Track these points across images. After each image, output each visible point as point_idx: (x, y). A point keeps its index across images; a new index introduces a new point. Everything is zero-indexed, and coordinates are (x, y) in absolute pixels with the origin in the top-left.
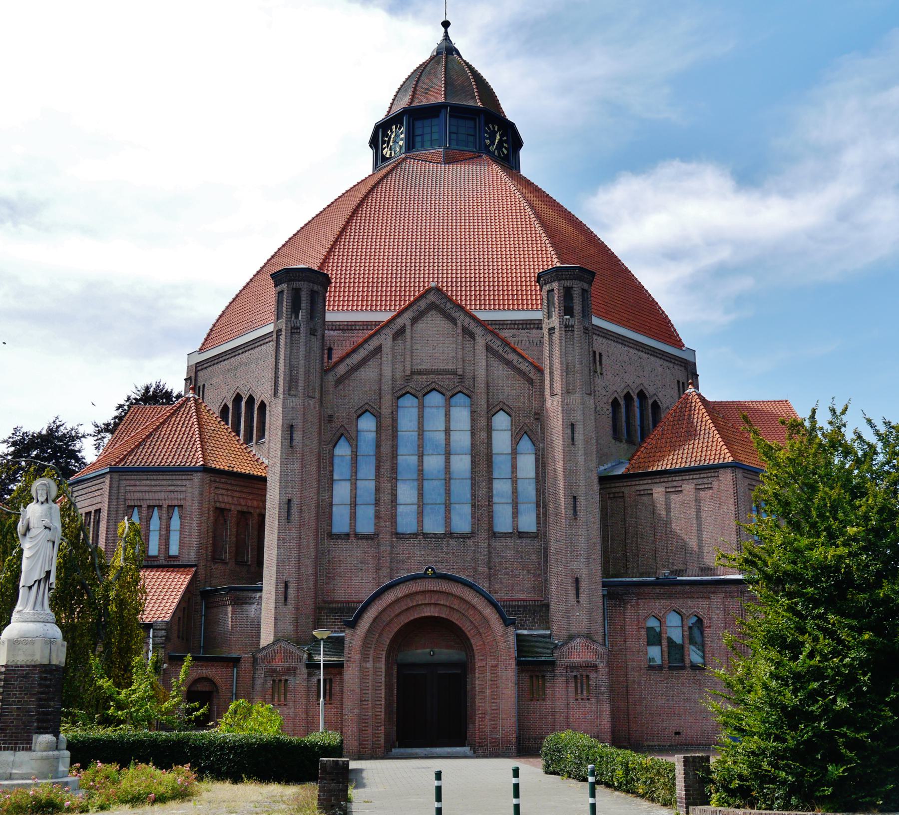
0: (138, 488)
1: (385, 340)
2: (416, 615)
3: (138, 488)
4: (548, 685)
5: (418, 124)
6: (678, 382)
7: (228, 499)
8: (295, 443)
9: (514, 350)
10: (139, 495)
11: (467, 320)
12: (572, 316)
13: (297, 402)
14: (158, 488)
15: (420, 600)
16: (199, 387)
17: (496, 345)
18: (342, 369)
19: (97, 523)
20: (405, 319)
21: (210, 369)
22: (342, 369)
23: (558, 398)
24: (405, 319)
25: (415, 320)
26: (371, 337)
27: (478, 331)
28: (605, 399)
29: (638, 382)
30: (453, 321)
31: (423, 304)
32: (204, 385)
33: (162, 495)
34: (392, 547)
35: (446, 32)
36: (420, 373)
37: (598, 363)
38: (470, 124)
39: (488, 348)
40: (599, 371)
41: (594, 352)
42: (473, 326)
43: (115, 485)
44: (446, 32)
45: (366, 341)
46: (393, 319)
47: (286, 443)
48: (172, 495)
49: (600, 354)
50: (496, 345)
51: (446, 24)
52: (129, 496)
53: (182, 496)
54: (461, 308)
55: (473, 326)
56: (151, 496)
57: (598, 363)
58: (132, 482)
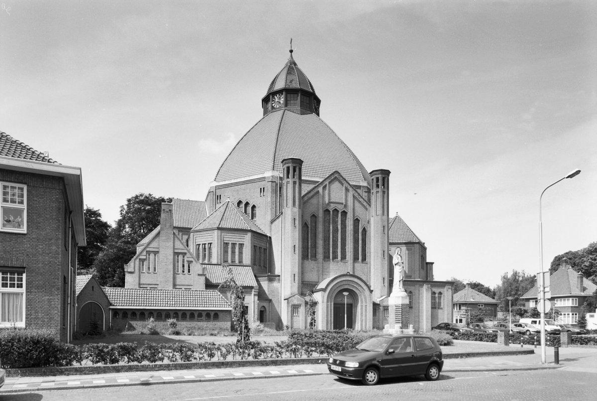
0: (227, 236)
1: (320, 189)
2: (343, 288)
3: (227, 236)
4: (377, 312)
7: (256, 242)
8: (296, 225)
9: (362, 198)
10: (228, 239)
11: (347, 184)
12: (378, 187)
13: (296, 210)
14: (235, 237)
15: (344, 283)
16: (218, 196)
17: (356, 195)
18: (306, 198)
20: (327, 182)
21: (223, 189)
22: (306, 198)
23: (380, 217)
24: (327, 182)
26: (316, 187)
27: (351, 189)
30: (342, 184)
32: (220, 196)
33: (237, 240)
34: (323, 263)
36: (331, 203)
38: (308, 98)
39: (354, 196)
42: (349, 187)
43: (220, 234)
45: (314, 189)
46: (323, 181)
47: (293, 225)
48: (240, 240)
50: (356, 195)
53: (244, 240)
54: (345, 180)
55: (349, 187)
56: (233, 239)
58: (225, 234)
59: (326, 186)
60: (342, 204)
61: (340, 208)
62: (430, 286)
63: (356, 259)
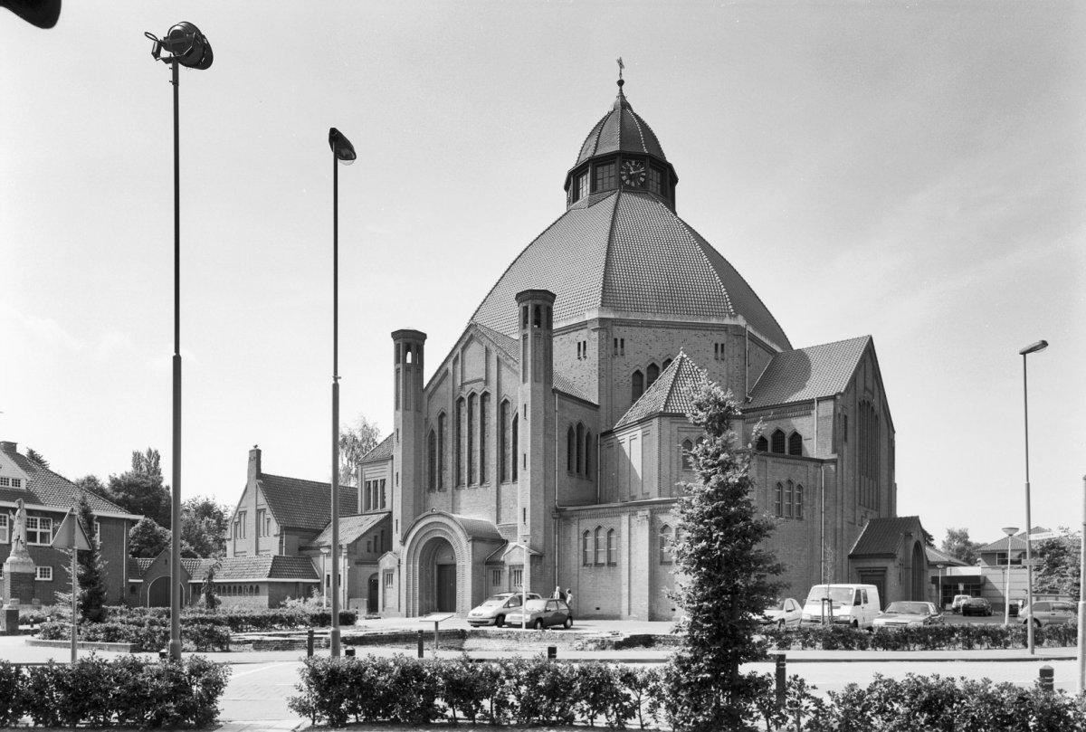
5: (600, 169)
6: (716, 345)
19: (383, 487)
25: (464, 349)
28: (626, 373)
29: (664, 354)
31: (467, 337)
35: (621, 90)
36: (467, 383)
37: (619, 347)
40: (619, 353)
41: (616, 340)
44: (621, 90)
49: (622, 340)
51: (621, 83)
52: (367, 476)
57: (619, 347)
59: (457, 356)
60: (480, 380)
61: (479, 388)
62: (647, 512)
63: (502, 478)
